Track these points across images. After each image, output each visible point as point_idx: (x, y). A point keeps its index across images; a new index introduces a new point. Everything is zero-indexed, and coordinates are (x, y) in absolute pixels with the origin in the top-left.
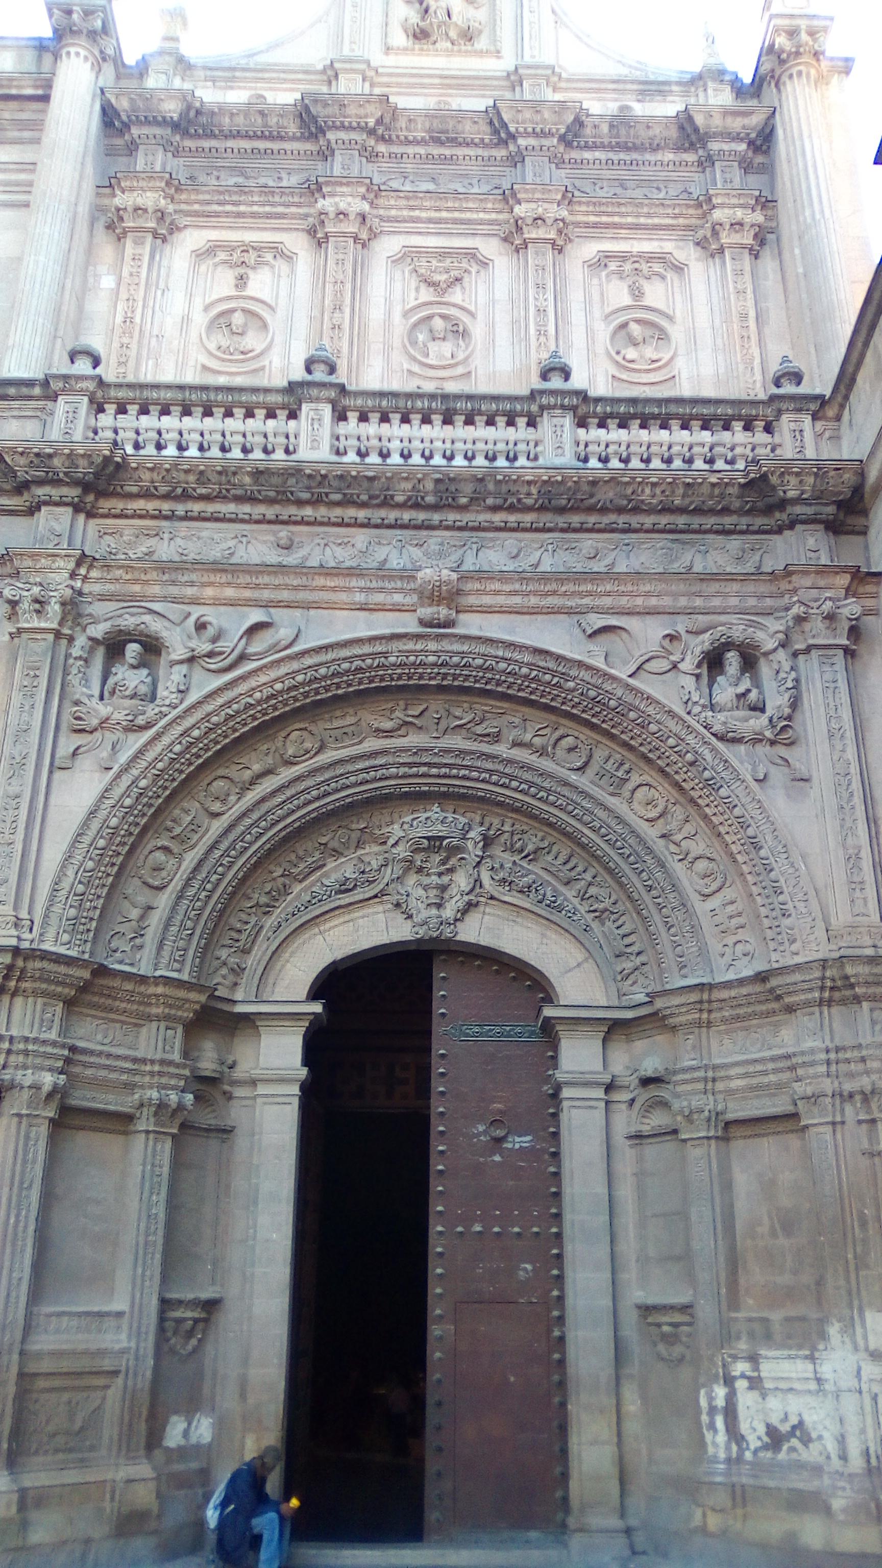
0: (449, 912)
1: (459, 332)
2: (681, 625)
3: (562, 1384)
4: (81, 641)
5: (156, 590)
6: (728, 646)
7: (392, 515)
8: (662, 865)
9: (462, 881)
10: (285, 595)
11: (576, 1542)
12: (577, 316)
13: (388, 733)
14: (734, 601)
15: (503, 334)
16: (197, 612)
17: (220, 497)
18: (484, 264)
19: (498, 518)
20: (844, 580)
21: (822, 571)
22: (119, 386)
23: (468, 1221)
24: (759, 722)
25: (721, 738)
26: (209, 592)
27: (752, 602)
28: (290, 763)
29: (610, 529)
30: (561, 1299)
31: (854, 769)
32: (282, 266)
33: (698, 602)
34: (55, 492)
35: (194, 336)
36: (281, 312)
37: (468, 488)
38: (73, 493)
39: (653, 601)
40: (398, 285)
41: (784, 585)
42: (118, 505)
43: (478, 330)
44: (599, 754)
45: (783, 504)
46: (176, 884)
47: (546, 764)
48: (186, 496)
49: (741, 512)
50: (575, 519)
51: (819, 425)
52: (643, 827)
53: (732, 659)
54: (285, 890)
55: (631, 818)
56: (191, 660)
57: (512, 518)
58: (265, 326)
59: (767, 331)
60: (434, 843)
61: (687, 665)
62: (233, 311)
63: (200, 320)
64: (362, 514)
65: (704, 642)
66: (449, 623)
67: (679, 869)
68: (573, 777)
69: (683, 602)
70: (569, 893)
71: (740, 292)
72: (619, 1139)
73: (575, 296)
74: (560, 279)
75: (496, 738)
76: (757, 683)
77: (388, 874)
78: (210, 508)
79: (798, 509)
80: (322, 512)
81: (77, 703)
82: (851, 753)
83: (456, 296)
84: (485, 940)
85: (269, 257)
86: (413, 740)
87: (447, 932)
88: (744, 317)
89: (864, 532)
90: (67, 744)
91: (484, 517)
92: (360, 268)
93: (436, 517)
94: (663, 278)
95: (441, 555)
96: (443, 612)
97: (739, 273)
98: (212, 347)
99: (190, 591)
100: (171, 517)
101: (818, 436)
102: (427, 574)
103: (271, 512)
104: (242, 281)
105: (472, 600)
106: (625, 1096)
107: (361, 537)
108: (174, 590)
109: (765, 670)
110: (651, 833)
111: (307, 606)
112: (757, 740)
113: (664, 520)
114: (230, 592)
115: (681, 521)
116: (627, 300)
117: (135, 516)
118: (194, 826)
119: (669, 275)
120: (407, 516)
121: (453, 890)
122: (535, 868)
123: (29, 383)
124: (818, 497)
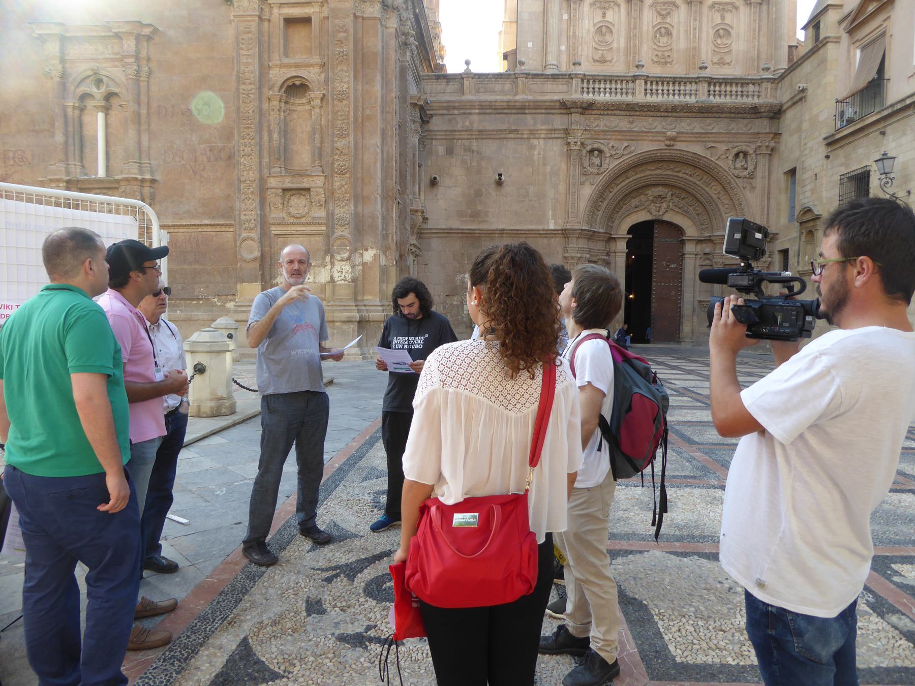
0: (661, 213)
1: (669, 33)
2: (730, 146)
3: (679, 316)
4: (584, 152)
5: (601, 137)
6: (741, 152)
7: (659, 114)
8: (717, 205)
9: (664, 205)
10: (633, 138)
11: (683, 343)
12: (704, 28)
13: (652, 170)
14: (744, 139)
15: (682, 36)
16: (612, 143)
17: (617, 110)
18: (677, 7)
19: (686, 115)
20: (772, 135)
21: (767, 133)
22: (589, 75)
23: (661, 283)
24: (746, 173)
25: (736, 177)
26: (614, 137)
27: (748, 140)
28: (628, 178)
29: (714, 117)
30: (680, 299)
31: (767, 186)
32: (616, 8)
33: (735, 140)
34: (576, 110)
35: (591, 37)
36: (616, 26)
37: (680, 108)
38: (580, 110)
39: (724, 139)
40: (651, 15)
41: (757, 136)
42: (590, 112)
43: (674, 32)
44: (705, 177)
45: (760, 113)
46: (603, 209)
47: (691, 178)
48: (608, 110)
49: (748, 113)
50: (706, 115)
51: (773, 85)
52: (713, 195)
53: (741, 154)
54: (622, 208)
55: (710, 193)
56: (611, 156)
57: (690, 114)
58: (611, 32)
59: (761, 33)
60: (660, 196)
61: (730, 158)
62: (602, 26)
63: (592, 30)
64: (651, 114)
65: (735, 151)
66: (673, 145)
67: (720, 206)
68: (697, 182)
69: (731, 139)
70: (691, 208)
71: (755, 21)
72: (697, 266)
73: (705, 19)
74: (701, 15)
75: (679, 172)
76: (746, 162)
77: (647, 203)
78: (613, 112)
79: (763, 114)
80: (642, 113)
81: (584, 168)
82: (766, 182)
83: (668, 20)
84: (669, 220)
85: (612, 4)
86: (658, 172)
87: (660, 218)
88: (755, 30)
89: (779, 119)
90: (583, 179)
91: (682, 114)
92: (641, 10)
93: (670, 114)
94: (731, 11)
95: (671, 124)
96: (672, 143)
97: (755, 13)
98: (596, 39)
99: (609, 137)
100: (603, 115)
101: (772, 88)
102: (669, 133)
103: (628, 113)
104: (604, 15)
105: (679, 139)
106: (699, 256)
107: (650, 119)
108: (605, 137)
109: (749, 158)
110: (715, 197)
111: (637, 140)
112: (745, 177)
113: (728, 115)
114: (619, 137)
115: (733, 115)
116: (719, 21)
117: (594, 114)
118: (607, 196)
119: (734, 10)
120: (663, 114)
121: (663, 208)
122: (683, 202)
123: (566, 75)
124: (769, 111)
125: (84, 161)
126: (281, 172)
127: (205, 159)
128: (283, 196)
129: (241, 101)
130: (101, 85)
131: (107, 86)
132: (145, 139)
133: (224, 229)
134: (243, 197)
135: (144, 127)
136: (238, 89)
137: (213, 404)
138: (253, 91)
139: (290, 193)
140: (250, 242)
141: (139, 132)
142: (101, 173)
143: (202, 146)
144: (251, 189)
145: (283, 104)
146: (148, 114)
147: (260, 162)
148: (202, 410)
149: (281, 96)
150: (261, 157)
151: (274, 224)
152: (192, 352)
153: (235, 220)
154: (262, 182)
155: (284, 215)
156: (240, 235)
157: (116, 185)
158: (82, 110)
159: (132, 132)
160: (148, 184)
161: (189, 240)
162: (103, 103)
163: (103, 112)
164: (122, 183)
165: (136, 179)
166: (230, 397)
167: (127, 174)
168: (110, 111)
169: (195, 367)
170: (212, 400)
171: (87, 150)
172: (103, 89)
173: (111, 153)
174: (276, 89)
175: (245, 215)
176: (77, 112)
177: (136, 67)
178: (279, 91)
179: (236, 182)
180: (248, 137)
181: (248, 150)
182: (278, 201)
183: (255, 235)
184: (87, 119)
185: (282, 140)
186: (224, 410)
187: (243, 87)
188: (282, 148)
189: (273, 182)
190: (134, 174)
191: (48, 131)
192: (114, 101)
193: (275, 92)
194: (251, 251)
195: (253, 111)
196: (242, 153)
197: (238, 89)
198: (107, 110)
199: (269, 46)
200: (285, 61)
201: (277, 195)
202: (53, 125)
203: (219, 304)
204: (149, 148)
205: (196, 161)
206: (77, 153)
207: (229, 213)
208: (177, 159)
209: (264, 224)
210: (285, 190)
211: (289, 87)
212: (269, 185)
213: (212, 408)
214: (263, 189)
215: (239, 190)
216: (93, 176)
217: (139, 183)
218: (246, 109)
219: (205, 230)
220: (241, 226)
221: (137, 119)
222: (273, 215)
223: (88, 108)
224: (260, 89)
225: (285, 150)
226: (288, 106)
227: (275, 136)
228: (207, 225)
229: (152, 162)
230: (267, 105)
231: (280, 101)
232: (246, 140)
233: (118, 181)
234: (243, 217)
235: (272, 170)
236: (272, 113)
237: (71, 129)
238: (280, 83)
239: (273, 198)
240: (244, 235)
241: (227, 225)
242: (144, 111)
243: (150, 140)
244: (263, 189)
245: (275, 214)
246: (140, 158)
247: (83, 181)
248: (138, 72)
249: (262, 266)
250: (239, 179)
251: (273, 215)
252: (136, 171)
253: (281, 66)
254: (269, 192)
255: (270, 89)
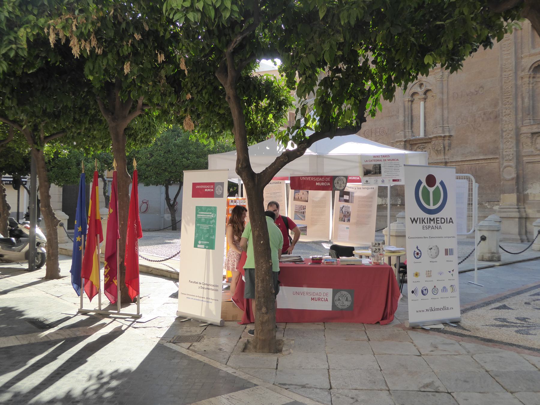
125: (413, 129)
126: (530, 123)
127: (481, 119)
128: (532, 137)
129: (503, 82)
130: (422, 86)
131: (426, 86)
132: (446, 112)
133: (492, 161)
134: (505, 140)
135: (445, 106)
136: (501, 75)
137: (489, 255)
138: (511, 75)
139: (537, 135)
140: (509, 168)
141: (443, 109)
142: (422, 135)
143: (479, 112)
144: (510, 136)
145: (531, 79)
146: (448, 98)
147: (516, 118)
148: (484, 258)
149: (530, 74)
150: (516, 115)
151: (526, 156)
152: (480, 230)
153: (500, 155)
154: (518, 129)
155: (532, 149)
156: (503, 164)
157: (430, 141)
158: (412, 101)
159: (439, 110)
160: (447, 138)
161: (471, 168)
162: (423, 96)
163: (423, 101)
164: (433, 139)
165: (441, 136)
166: (498, 253)
167: (435, 134)
168: (427, 100)
169: (481, 237)
170: (489, 253)
171: (415, 122)
172: (424, 89)
173: (427, 123)
174: (527, 70)
175: (506, 152)
176: (410, 103)
177: (441, 74)
178: (529, 71)
179: (500, 132)
180: (508, 103)
181: (508, 112)
182: (529, 141)
183: (513, 163)
184: (415, 106)
185: (531, 102)
186: (495, 259)
187: (505, 73)
188: (531, 107)
189: (524, 130)
190: (439, 134)
191: (396, 115)
192: (429, 94)
193: (526, 73)
194: (510, 174)
195: (511, 87)
196: (504, 114)
197: (501, 75)
198: (425, 99)
199: (522, 44)
200: (533, 51)
201: (527, 137)
202: (398, 112)
203: (489, 207)
204: (448, 117)
205: (475, 122)
206: (410, 125)
207: (496, 151)
208: (464, 122)
209: (518, 157)
210: (533, 134)
211: (536, 67)
212: (522, 132)
213: (489, 257)
214: (518, 135)
215: (502, 136)
216: (418, 137)
217: (442, 139)
218: (507, 87)
219: (480, 162)
220: (503, 158)
221: (442, 103)
222: (525, 150)
223: (415, 100)
224: (516, 73)
225: (534, 107)
226: (535, 79)
227: (526, 100)
228: (482, 159)
229: (450, 125)
230: (520, 81)
231: (529, 78)
232: (507, 106)
233: (431, 139)
234: (504, 153)
235: (524, 122)
236: (524, 86)
237: (407, 113)
238: (529, 66)
239: (523, 139)
240: (505, 164)
241: (494, 158)
242: (445, 97)
243: (448, 112)
244: (518, 135)
245: (527, 149)
246: (443, 124)
247: (413, 140)
248: (442, 76)
249: (517, 183)
250: (502, 130)
251: (525, 150)
252: (441, 132)
253: (530, 55)
254: (522, 136)
255: (522, 71)
